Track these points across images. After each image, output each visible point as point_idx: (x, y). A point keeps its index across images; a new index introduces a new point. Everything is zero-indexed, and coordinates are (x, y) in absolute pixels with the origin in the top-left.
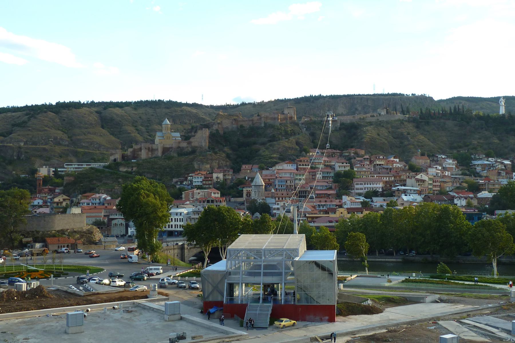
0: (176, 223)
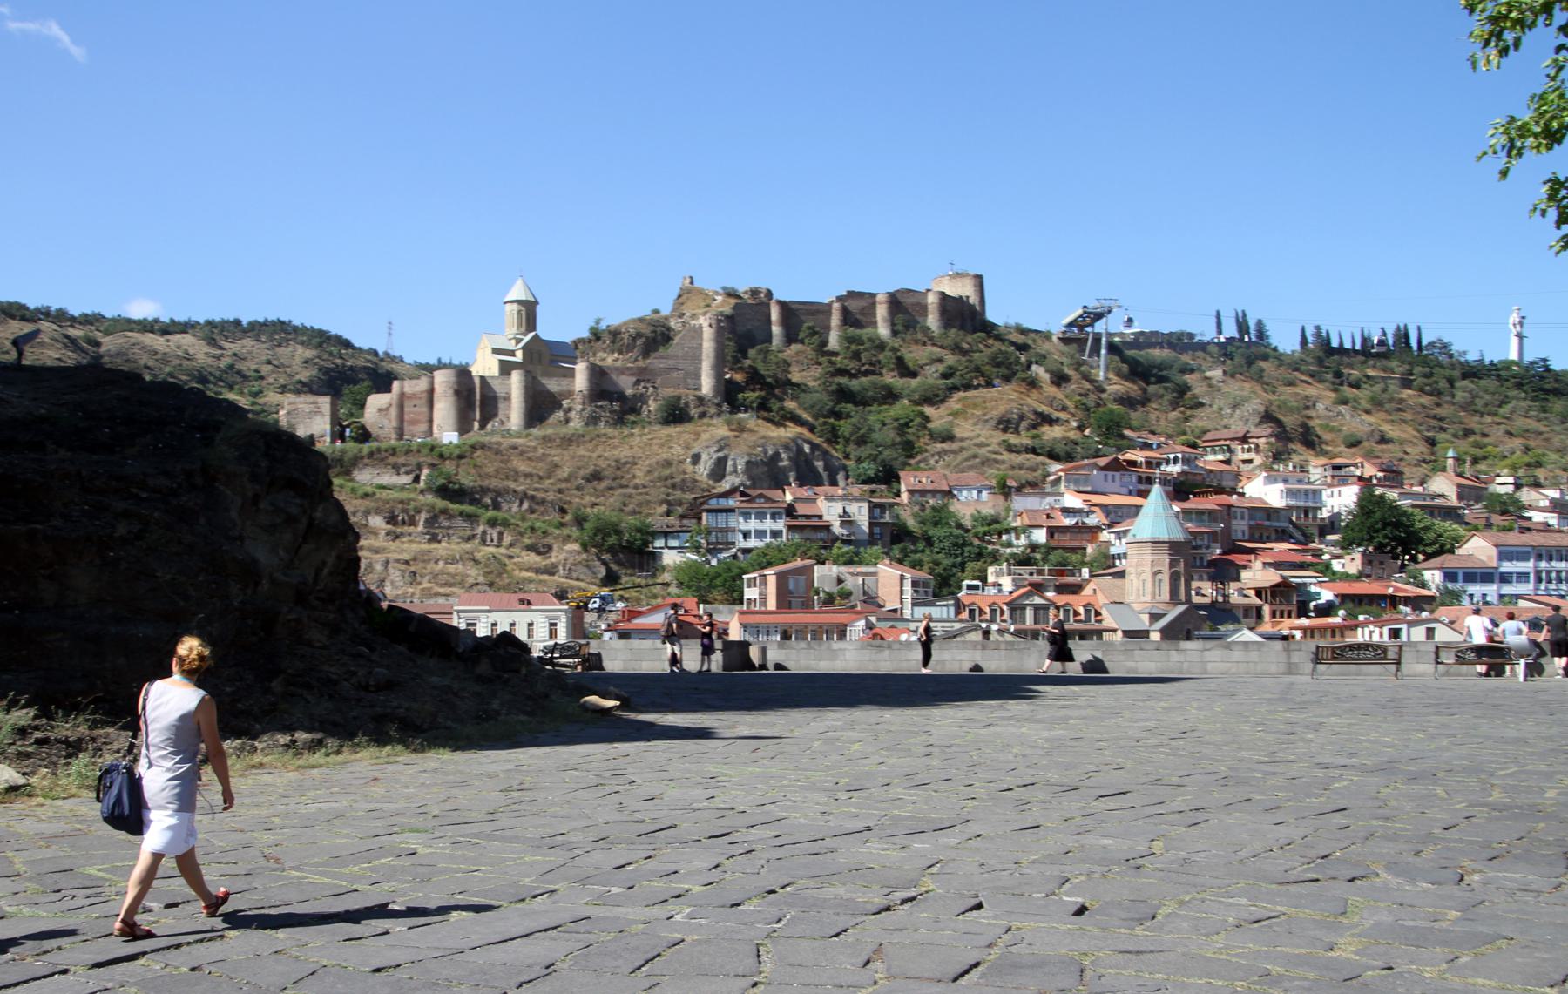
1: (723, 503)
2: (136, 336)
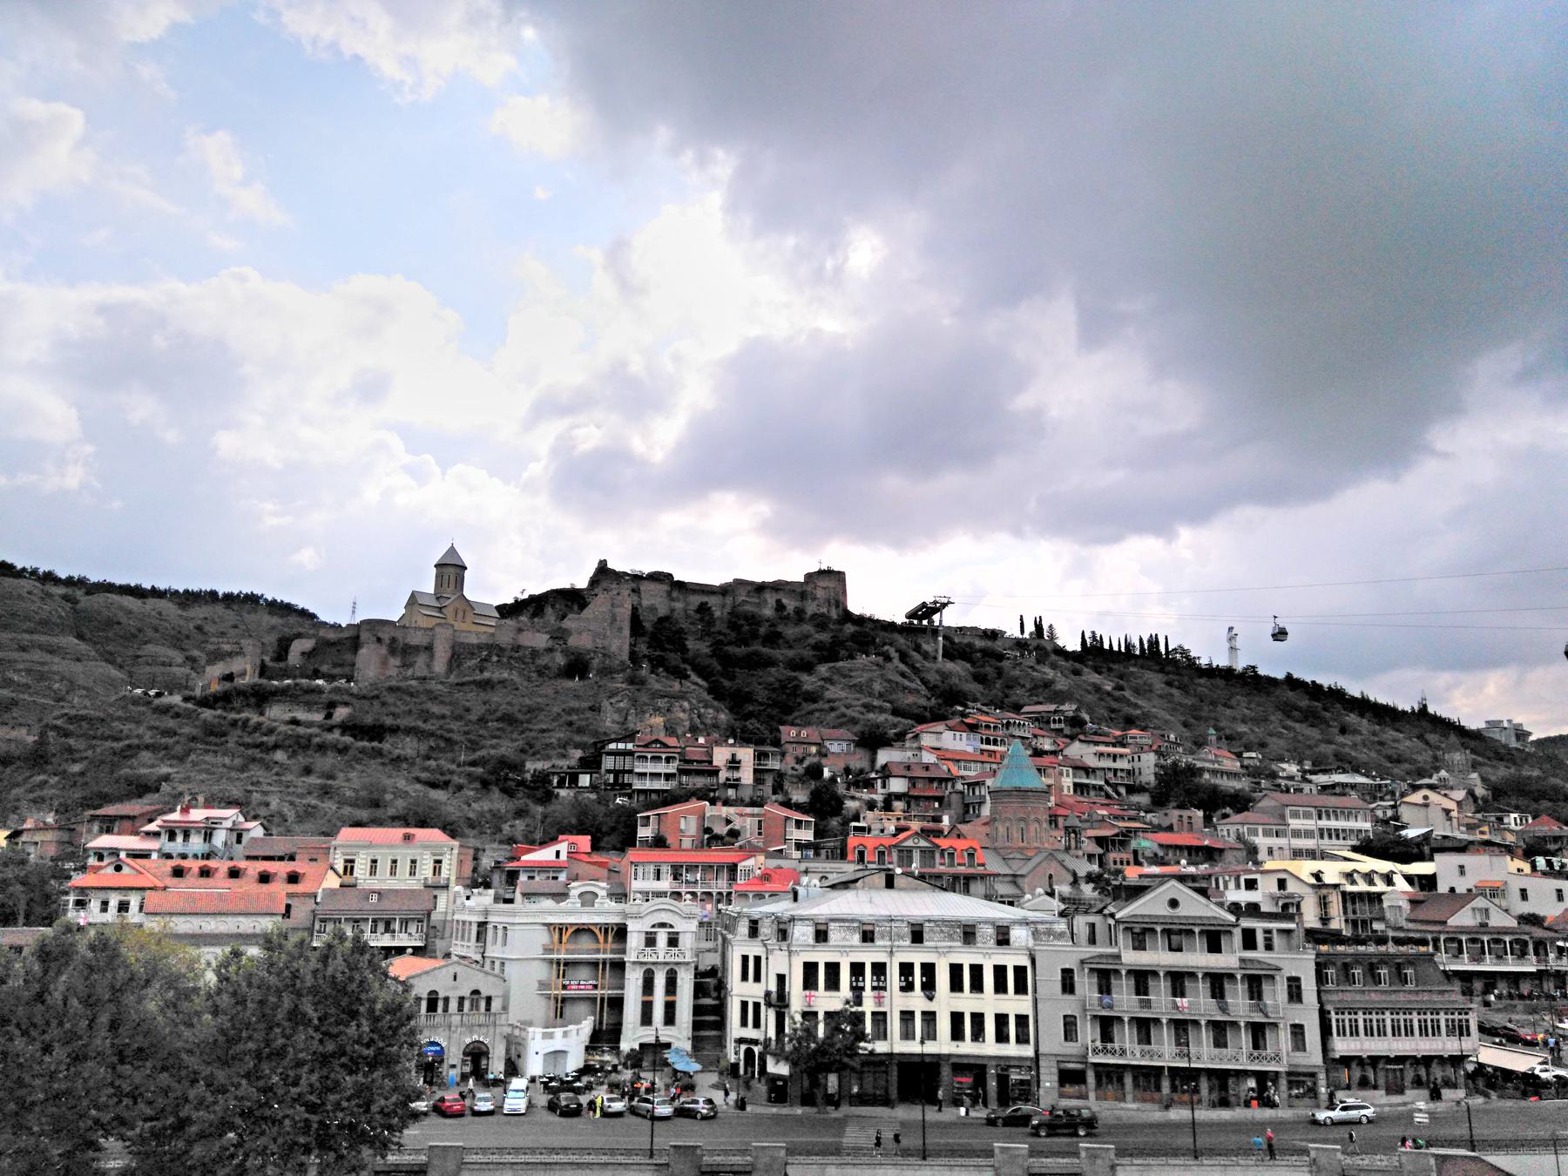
0: (967, 1003)
1: (621, 746)
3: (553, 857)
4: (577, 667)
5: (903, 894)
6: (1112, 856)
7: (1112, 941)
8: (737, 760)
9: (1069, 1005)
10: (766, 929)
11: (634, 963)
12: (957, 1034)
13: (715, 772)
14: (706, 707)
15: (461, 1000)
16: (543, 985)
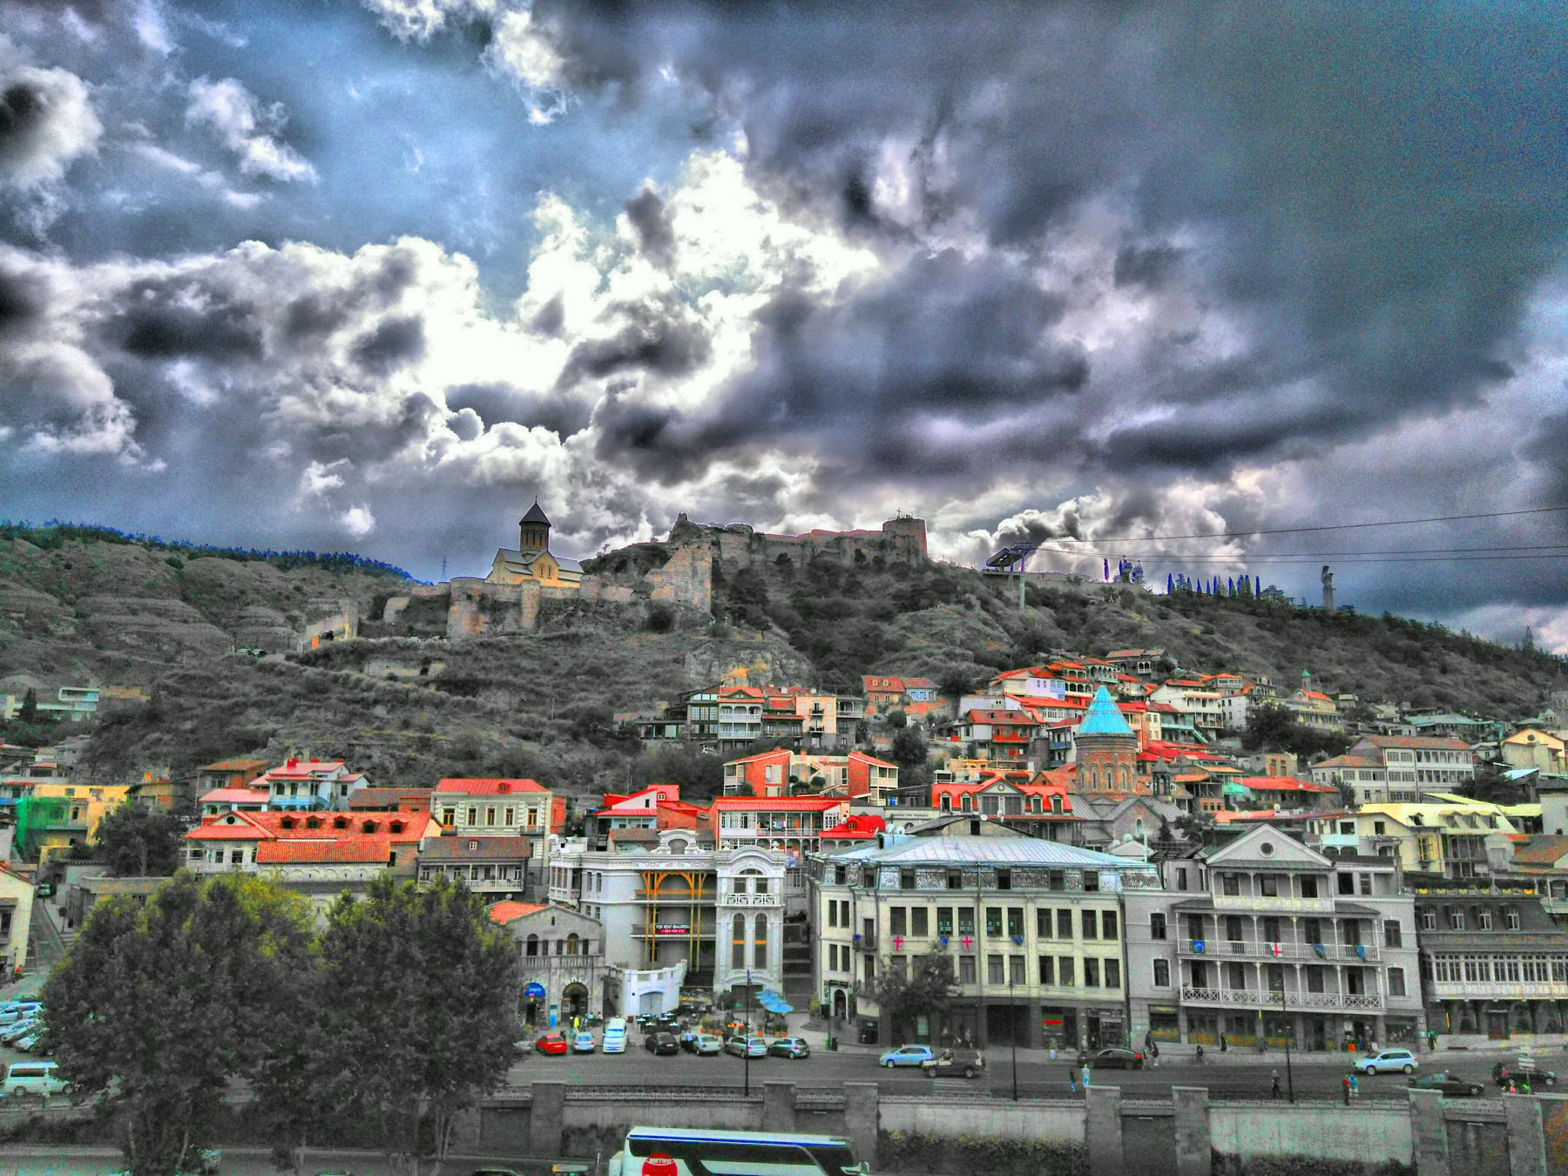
0: (1055, 948)
1: (706, 697)
2: (216, 561)
3: (643, 806)
4: (660, 621)
5: (989, 840)
6: (1202, 801)
7: (1203, 887)
8: (820, 709)
9: (1158, 950)
10: (853, 875)
11: (725, 908)
12: (1045, 977)
13: (799, 722)
14: (788, 657)
15: (560, 943)
16: (637, 929)
